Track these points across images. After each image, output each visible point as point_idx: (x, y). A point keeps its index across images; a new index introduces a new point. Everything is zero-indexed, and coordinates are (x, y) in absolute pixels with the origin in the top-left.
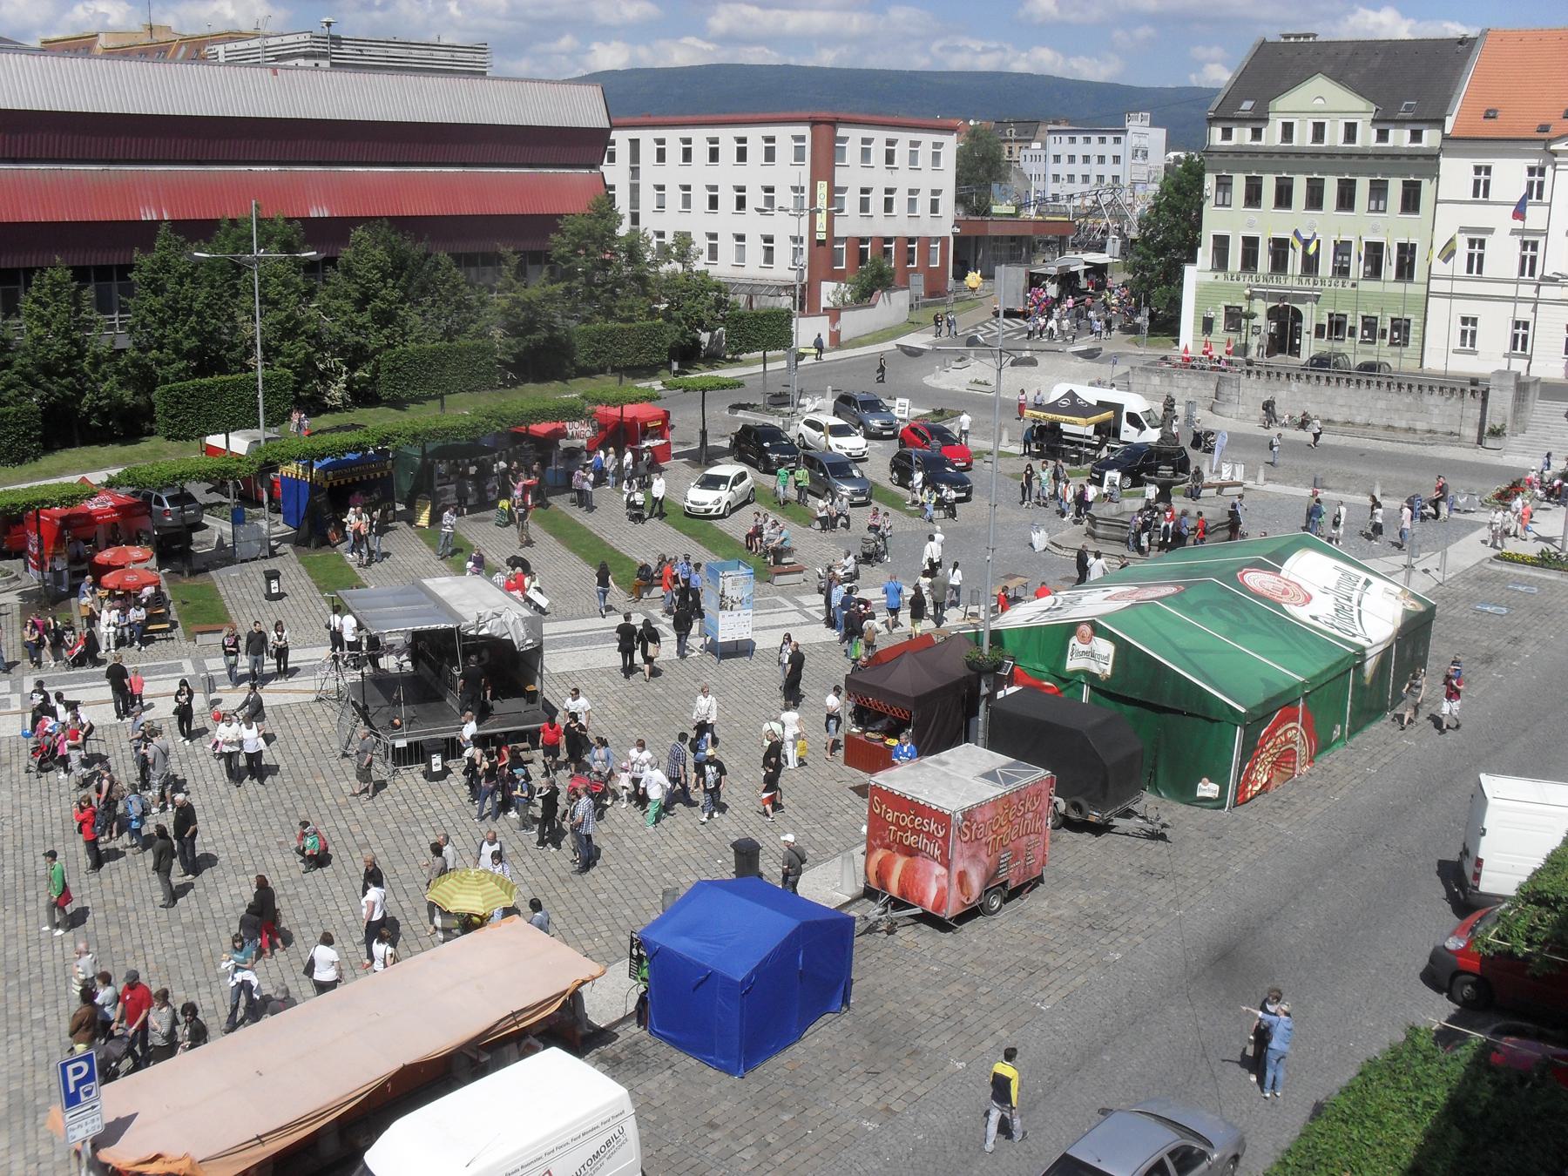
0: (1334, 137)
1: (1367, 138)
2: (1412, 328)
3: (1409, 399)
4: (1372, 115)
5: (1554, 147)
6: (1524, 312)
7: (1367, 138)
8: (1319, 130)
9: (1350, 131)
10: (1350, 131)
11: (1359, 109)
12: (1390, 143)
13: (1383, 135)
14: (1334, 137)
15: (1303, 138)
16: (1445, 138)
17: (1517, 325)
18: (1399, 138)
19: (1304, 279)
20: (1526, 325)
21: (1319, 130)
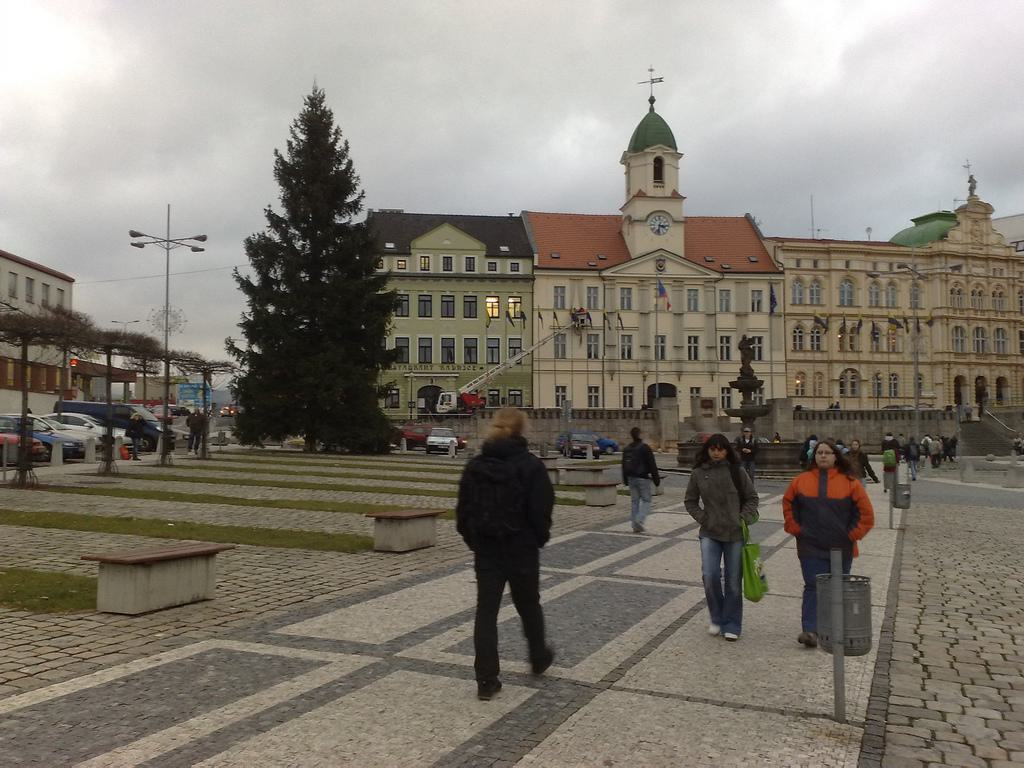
0: (459, 266)
1: (481, 266)
2: (525, 395)
3: (602, 423)
4: (484, 253)
5: (604, 274)
6: (595, 381)
7: (481, 266)
8: (448, 262)
9: (470, 262)
10: (470, 262)
11: (474, 247)
12: (498, 272)
13: (493, 266)
14: (459, 266)
15: (437, 267)
16: (535, 268)
17: (590, 389)
18: (504, 267)
19: (445, 366)
20: (597, 389)
21: (448, 262)
